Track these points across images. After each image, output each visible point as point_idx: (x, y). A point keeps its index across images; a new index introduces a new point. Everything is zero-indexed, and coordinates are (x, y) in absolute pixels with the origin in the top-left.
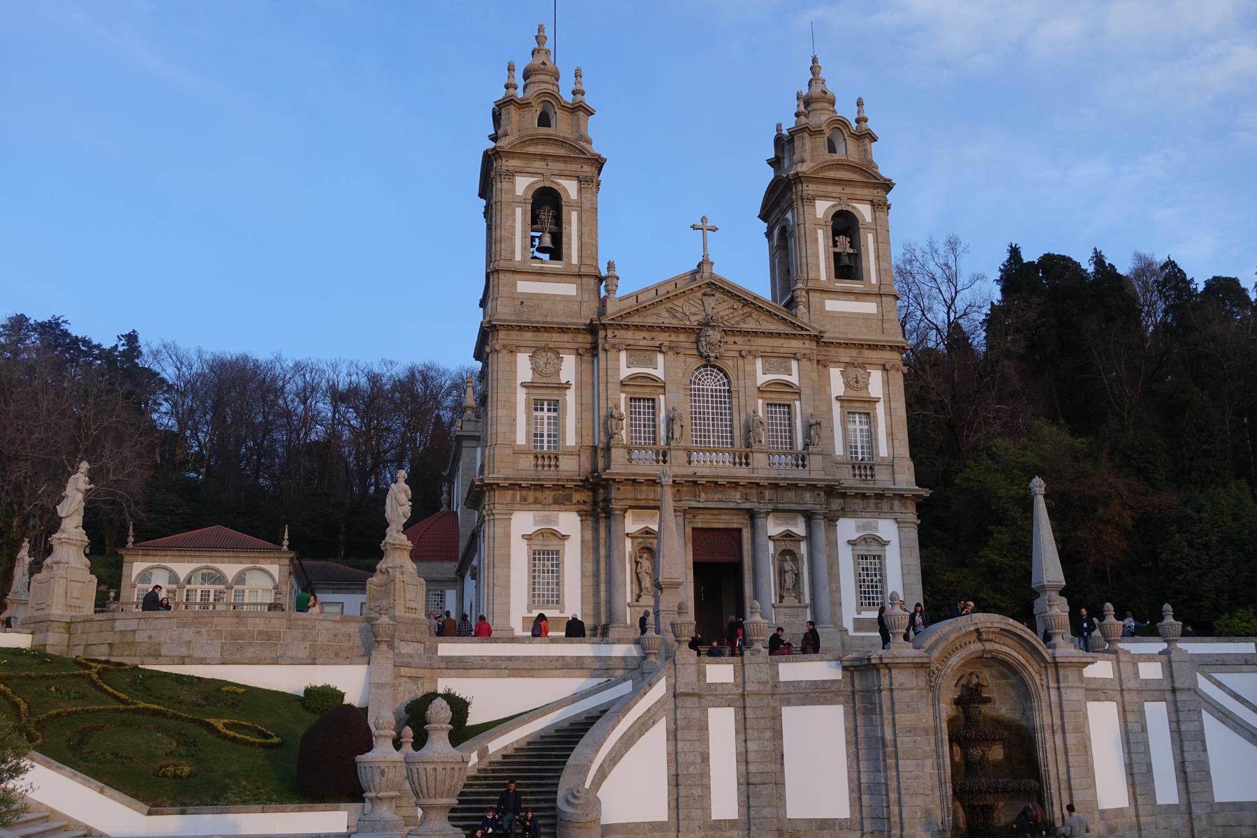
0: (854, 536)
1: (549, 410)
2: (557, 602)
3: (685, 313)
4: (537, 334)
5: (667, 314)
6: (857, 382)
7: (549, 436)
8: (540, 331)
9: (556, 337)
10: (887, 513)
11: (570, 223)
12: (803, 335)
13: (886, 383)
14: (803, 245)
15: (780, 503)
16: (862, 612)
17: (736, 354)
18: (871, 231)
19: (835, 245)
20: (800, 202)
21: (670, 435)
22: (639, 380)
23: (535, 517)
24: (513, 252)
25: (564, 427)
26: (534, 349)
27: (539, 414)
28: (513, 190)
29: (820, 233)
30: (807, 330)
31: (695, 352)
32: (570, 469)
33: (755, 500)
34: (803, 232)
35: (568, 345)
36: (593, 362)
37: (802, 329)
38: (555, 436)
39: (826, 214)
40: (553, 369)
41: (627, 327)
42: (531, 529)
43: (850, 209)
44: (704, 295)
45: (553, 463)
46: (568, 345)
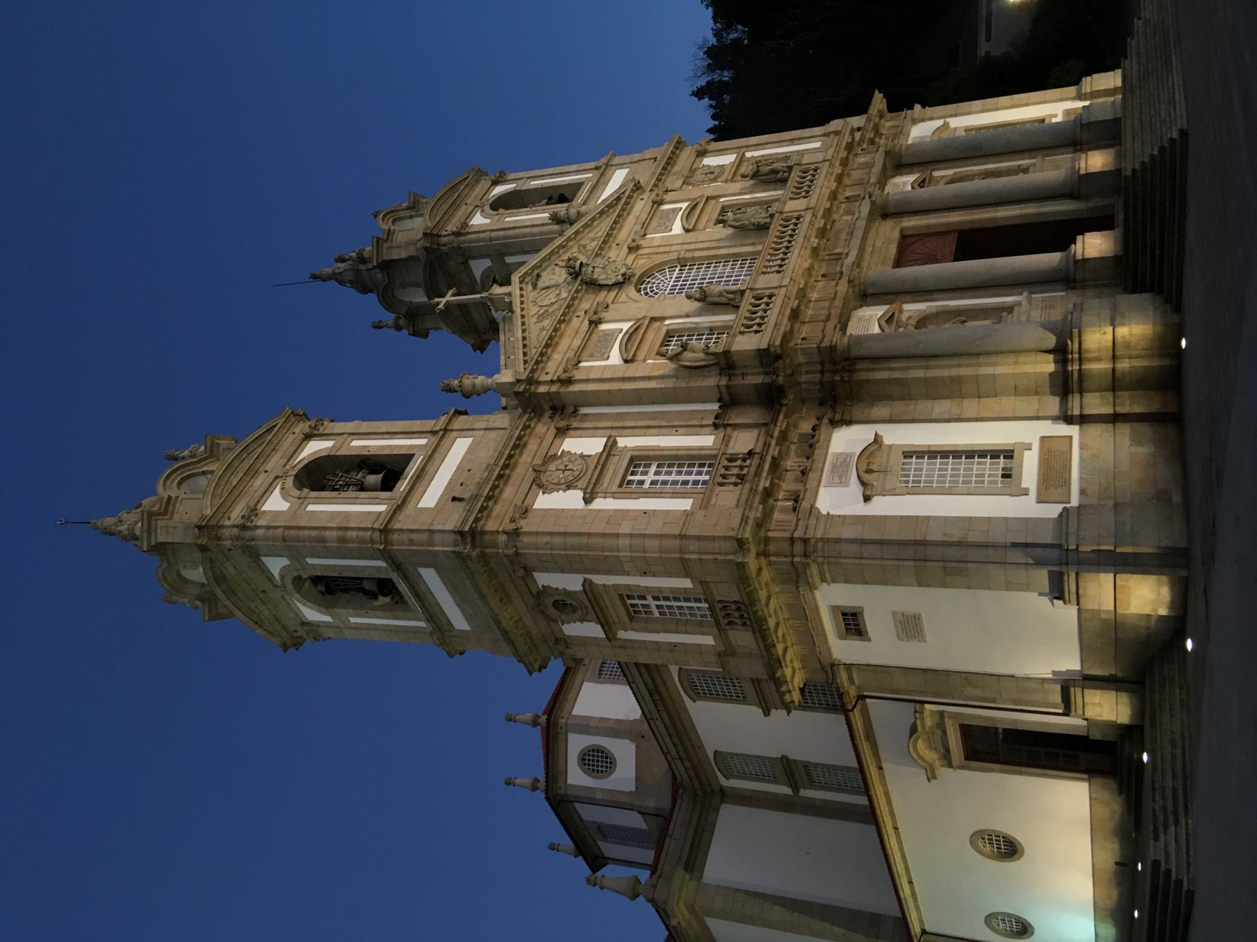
1: (645, 473)
2: (1009, 454)
3: (554, 303)
4: (511, 481)
8: (509, 476)
9: (526, 459)
11: (364, 447)
12: (630, 197)
14: (517, 231)
17: (631, 257)
20: (462, 238)
22: (629, 346)
23: (830, 485)
24: (370, 513)
25: (679, 449)
26: (534, 487)
27: (647, 485)
28: (277, 514)
30: (623, 193)
31: (613, 294)
32: (755, 440)
33: (857, 203)
34: (501, 233)
35: (546, 443)
36: (586, 415)
37: (619, 199)
40: (580, 461)
41: (543, 356)
42: (855, 488)
43: (494, 199)
44: (535, 286)
45: (739, 463)
46: (546, 443)
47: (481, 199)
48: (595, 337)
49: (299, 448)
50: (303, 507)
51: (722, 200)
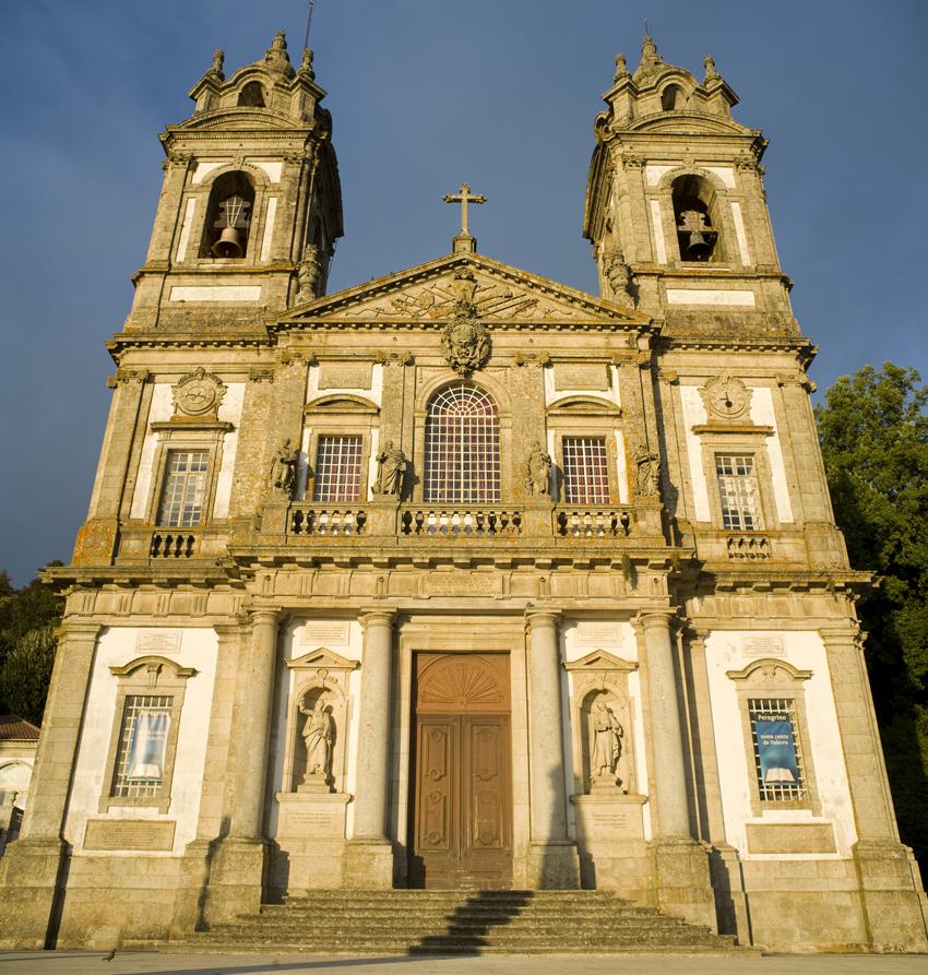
0: (739, 664)
5: (394, 309)
6: (729, 404)
7: (189, 508)
10: (798, 619)
11: (263, 213)
12: (621, 327)
13: (783, 408)
15: (581, 598)
16: (764, 812)
17: (512, 362)
18: (736, 199)
19: (679, 221)
21: (376, 489)
29: (655, 206)
37: (620, 316)
38: (197, 509)
39: (663, 179)
43: (699, 173)
47: (696, 161)
48: (362, 367)
49: (273, 156)
50: (191, 195)
51: (618, 434)
